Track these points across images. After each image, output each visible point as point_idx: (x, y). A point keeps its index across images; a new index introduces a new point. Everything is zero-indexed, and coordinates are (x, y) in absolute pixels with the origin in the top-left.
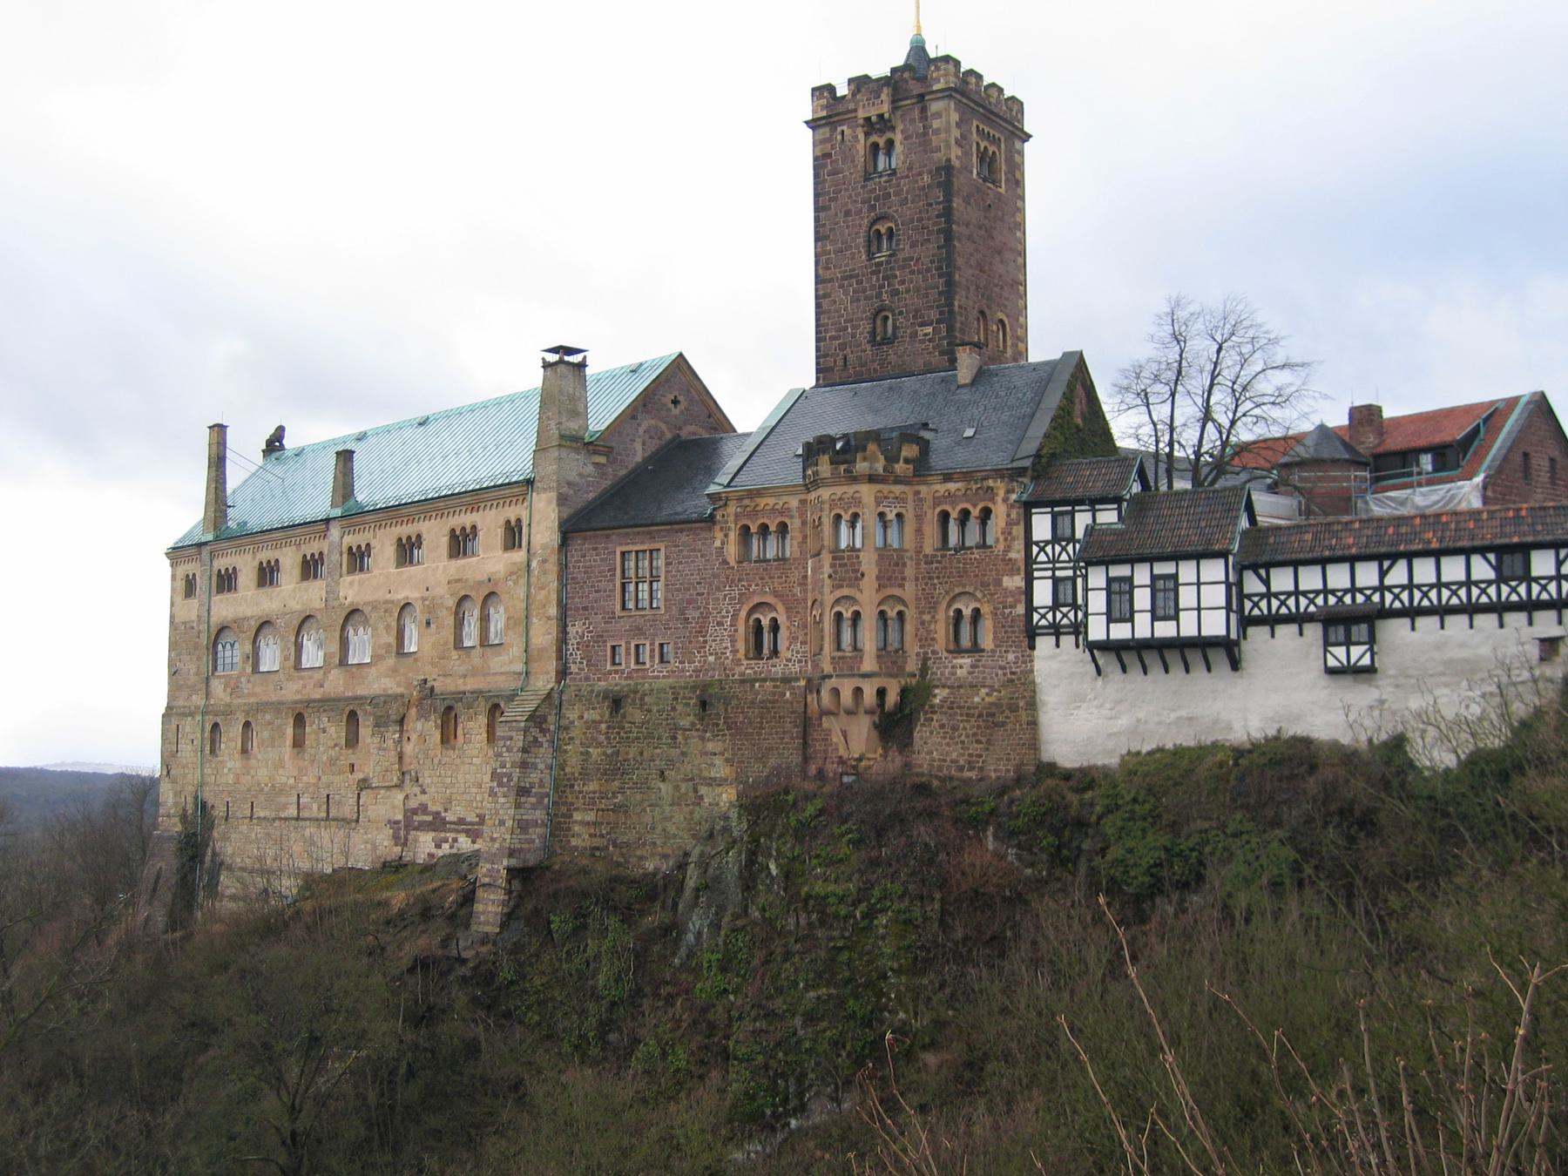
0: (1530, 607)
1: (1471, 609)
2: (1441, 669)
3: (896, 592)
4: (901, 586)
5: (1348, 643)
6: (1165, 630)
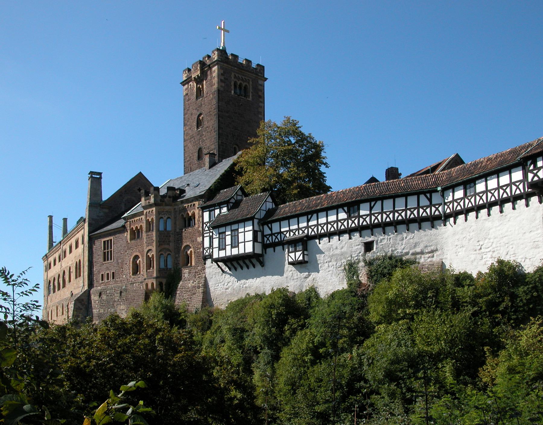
0: (360, 229)
1: (340, 233)
2: (329, 259)
3: (167, 246)
4: (169, 244)
5: (295, 251)
6: (235, 252)
